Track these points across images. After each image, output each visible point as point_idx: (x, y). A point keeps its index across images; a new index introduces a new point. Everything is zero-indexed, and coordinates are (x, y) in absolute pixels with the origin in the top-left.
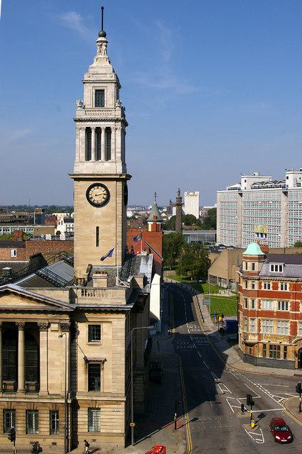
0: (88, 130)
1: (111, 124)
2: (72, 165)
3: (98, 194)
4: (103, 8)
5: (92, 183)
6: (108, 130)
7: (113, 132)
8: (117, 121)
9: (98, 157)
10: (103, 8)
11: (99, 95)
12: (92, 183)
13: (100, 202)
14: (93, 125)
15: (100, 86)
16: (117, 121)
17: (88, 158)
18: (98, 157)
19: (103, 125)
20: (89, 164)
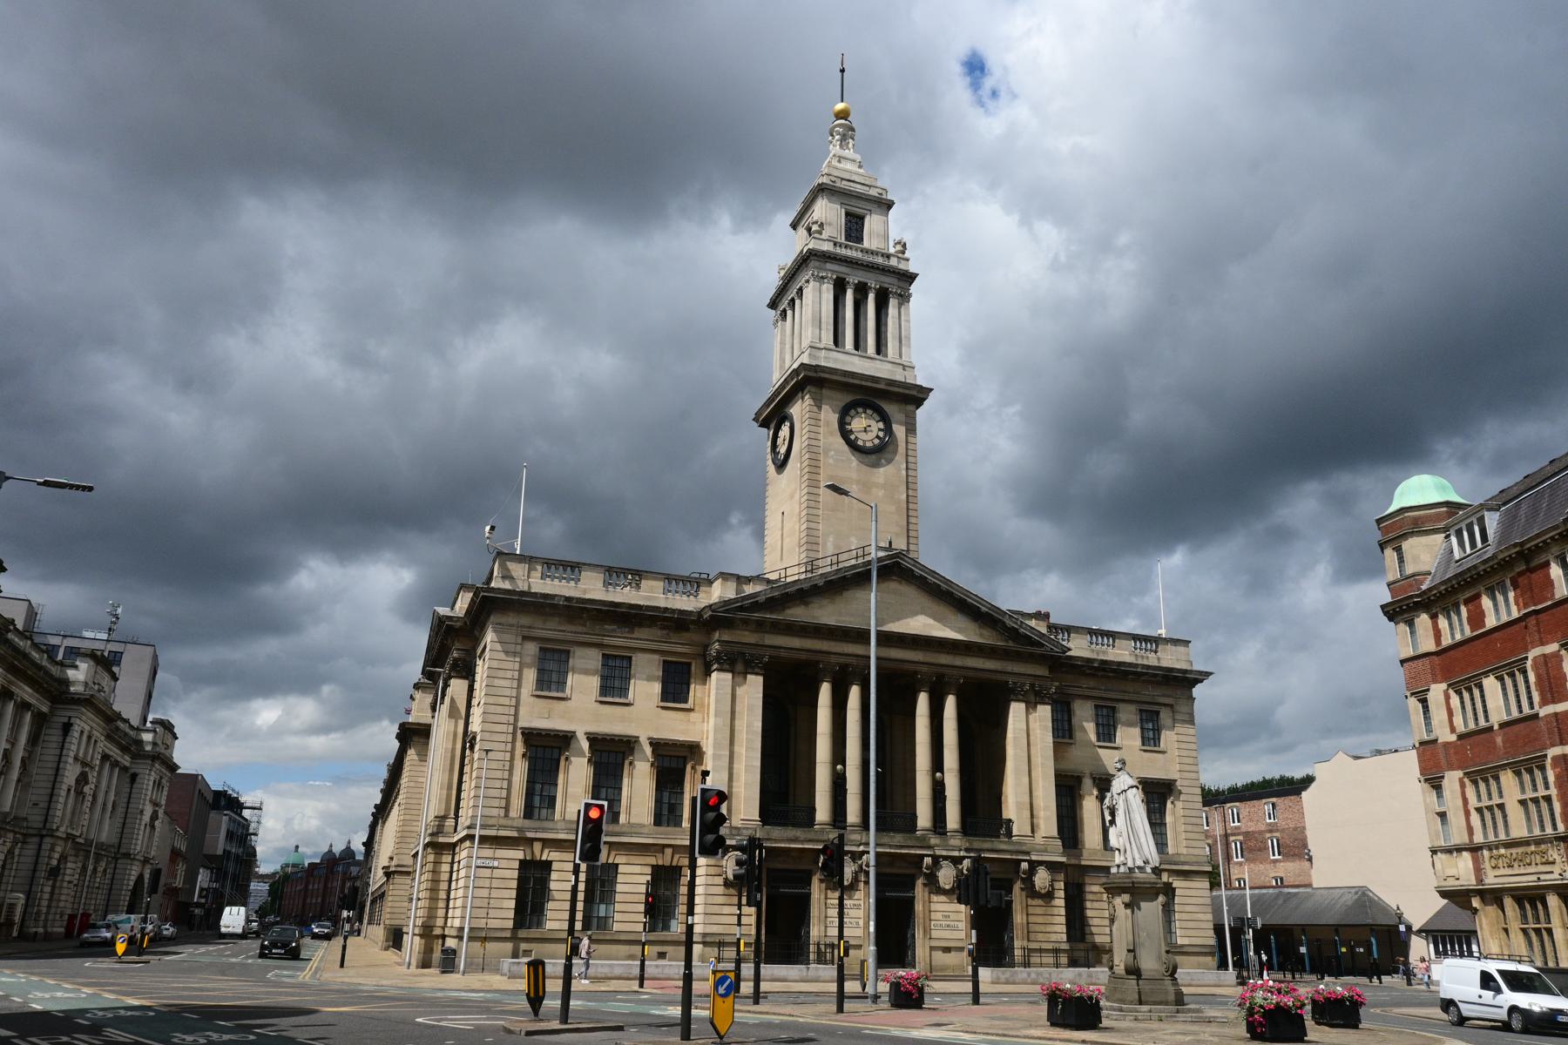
1: (888, 281)
3: (865, 427)
4: (843, 71)
13: (869, 444)
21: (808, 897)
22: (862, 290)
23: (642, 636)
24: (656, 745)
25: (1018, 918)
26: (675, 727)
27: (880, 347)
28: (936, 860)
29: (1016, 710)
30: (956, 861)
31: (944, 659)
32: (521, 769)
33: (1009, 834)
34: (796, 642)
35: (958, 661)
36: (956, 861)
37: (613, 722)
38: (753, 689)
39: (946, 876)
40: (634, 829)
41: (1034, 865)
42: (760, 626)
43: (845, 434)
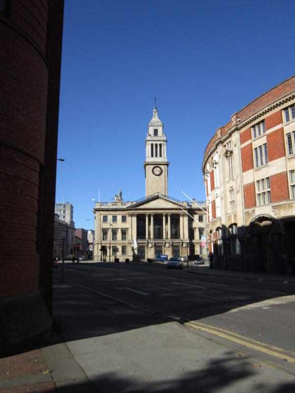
0: (152, 145)
2: (145, 159)
3: (157, 171)
4: (155, 98)
5: (154, 166)
6: (161, 145)
7: (162, 145)
8: (164, 141)
9: (156, 156)
10: (155, 98)
11: (156, 132)
12: (154, 166)
14: (154, 143)
15: (156, 128)
16: (164, 141)
17: (152, 156)
18: (156, 156)
19: (158, 143)
20: (152, 158)
21: (162, 250)
22: (156, 145)
23: (118, 212)
24: (121, 229)
25: (180, 251)
26: (124, 225)
27: (161, 156)
28: (165, 243)
29: (181, 218)
30: (169, 243)
31: (168, 211)
32: (102, 234)
33: (179, 238)
34: (141, 211)
35: (170, 211)
36: (169, 243)
37: (115, 226)
38: (135, 219)
39: (167, 245)
40: (120, 241)
41: (183, 243)
42: (135, 210)
43: (153, 173)
